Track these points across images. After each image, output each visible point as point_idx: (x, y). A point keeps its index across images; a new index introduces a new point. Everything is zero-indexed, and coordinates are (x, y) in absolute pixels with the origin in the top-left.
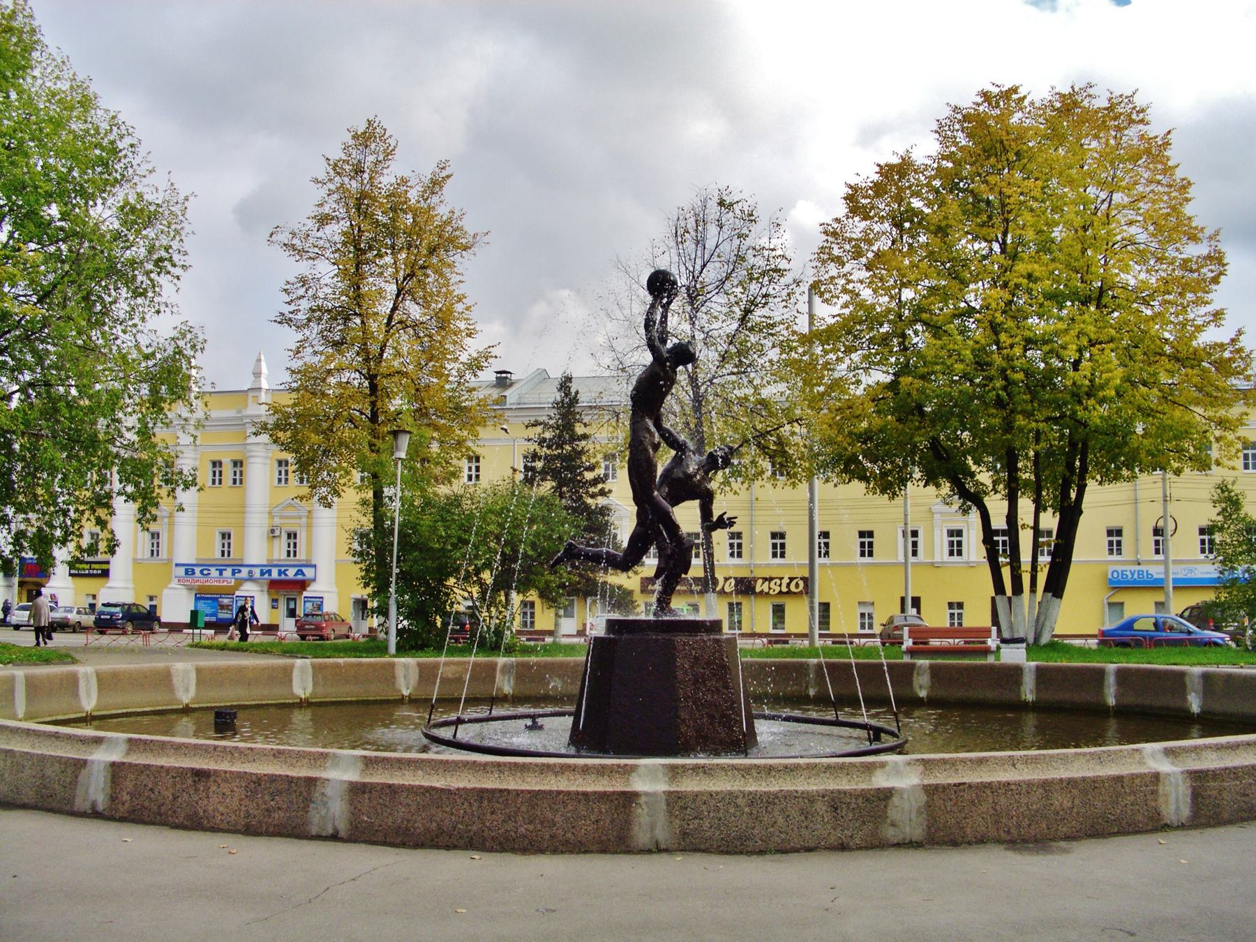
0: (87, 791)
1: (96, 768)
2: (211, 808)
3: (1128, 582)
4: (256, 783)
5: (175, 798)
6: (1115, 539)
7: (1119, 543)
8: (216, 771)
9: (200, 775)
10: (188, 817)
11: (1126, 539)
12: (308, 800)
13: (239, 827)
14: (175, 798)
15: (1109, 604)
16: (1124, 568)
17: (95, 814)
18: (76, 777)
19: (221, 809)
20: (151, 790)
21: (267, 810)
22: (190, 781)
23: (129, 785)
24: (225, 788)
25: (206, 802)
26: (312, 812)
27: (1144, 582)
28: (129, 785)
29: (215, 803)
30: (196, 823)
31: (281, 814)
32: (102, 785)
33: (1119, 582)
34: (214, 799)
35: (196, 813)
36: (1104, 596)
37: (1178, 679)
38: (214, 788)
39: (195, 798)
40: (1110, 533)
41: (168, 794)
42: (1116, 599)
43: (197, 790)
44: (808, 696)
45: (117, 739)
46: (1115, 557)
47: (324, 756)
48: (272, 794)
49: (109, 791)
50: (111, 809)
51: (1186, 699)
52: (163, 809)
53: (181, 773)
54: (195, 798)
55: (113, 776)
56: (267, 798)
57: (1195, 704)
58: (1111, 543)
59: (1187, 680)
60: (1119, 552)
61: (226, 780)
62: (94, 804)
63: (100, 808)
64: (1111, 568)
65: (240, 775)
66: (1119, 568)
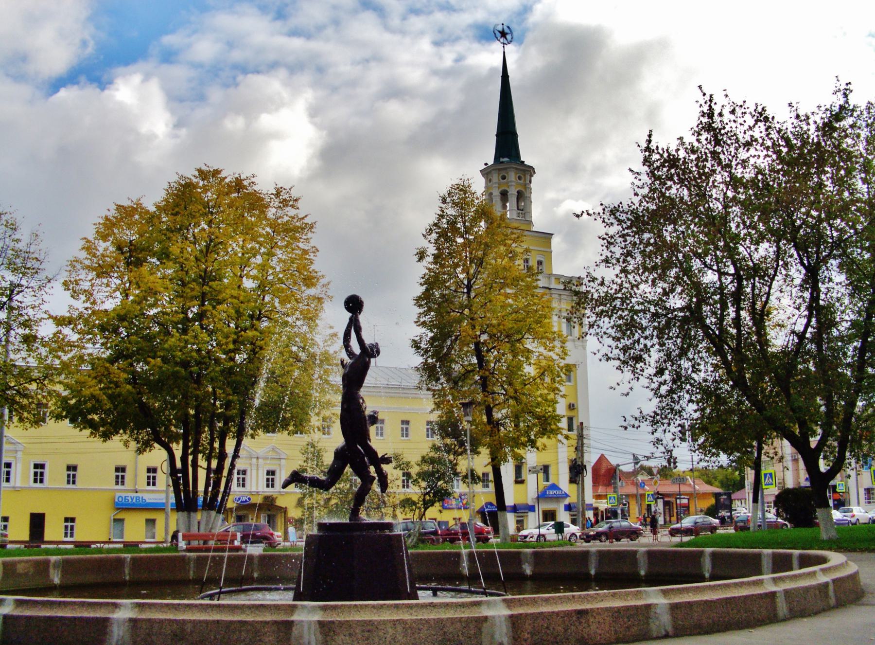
0: (492, 636)
1: (497, 621)
5: (566, 630)
6: (120, 474)
7: (123, 477)
8: (591, 609)
9: (581, 613)
11: (128, 475)
12: (648, 618)
18: (480, 629)
20: (547, 628)
23: (528, 627)
26: (652, 624)
28: (528, 627)
33: (122, 504)
34: (593, 627)
35: (583, 637)
36: (112, 514)
40: (117, 469)
41: (560, 629)
42: (118, 517)
43: (580, 623)
46: (120, 487)
51: (521, 568)
53: (568, 614)
54: (580, 628)
56: (626, 620)
57: (528, 570)
58: (117, 477)
59: (522, 557)
60: (123, 483)
64: (118, 494)
65: (607, 609)
66: (124, 495)
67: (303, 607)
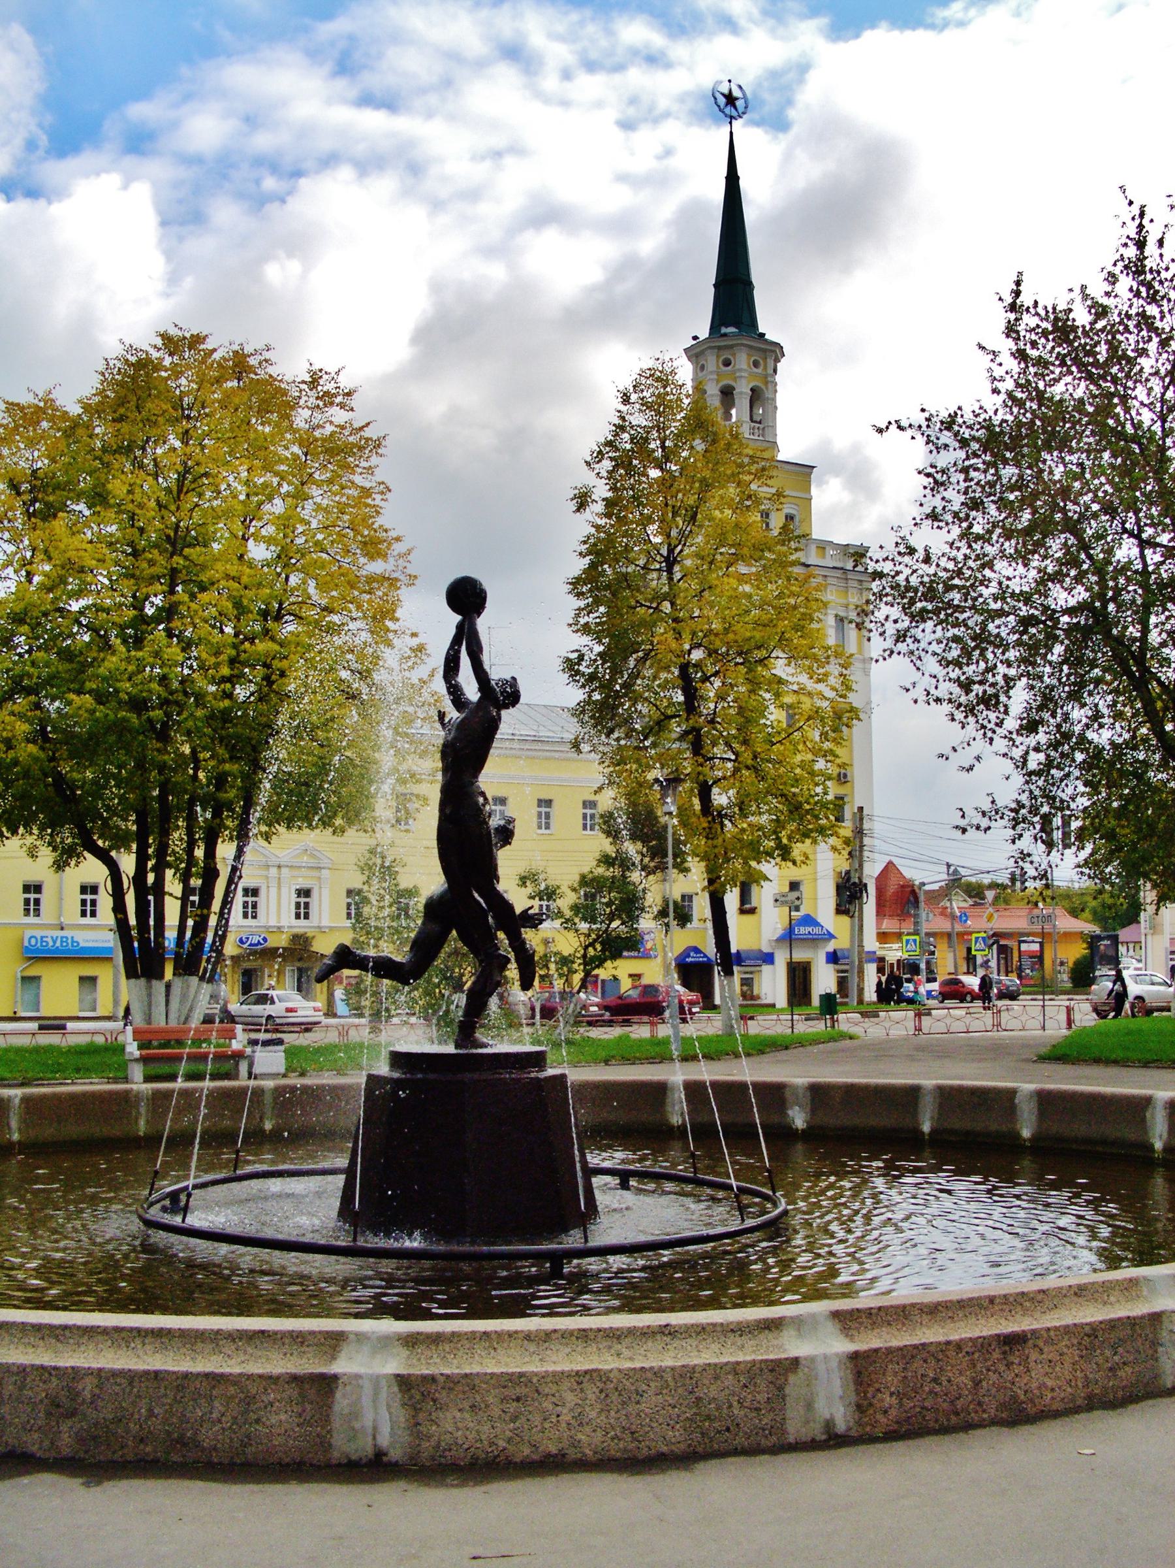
0: (809, 1406)
1: (821, 1368)
2: (1034, 1385)
3: (49, 951)
4: (1091, 1335)
5: (977, 1383)
6: (32, 896)
7: (37, 902)
8: (1034, 1331)
9: (1012, 1341)
10: (1003, 1406)
11: (46, 897)
12: (1155, 1344)
13: (1079, 1402)
14: (977, 1383)
15: (23, 978)
16: (44, 933)
17: (834, 1440)
18: (780, 1389)
19: (1050, 1383)
20: (935, 1380)
21: (1111, 1369)
22: (996, 1355)
23: (891, 1380)
24: (1050, 1353)
25: (1026, 1379)
26: (1163, 1359)
27: (69, 951)
28: (891, 1380)
29: (1042, 1377)
30: (1019, 1415)
31: (1128, 1369)
32: (839, 1392)
33: (38, 951)
34: (1038, 1372)
35: (1014, 1398)
36: (18, 968)
37: (660, 1090)
38: (1034, 1355)
39: (1009, 1376)
40: (27, 888)
41: (965, 1380)
42: (32, 972)
43: (1009, 1365)
44: (263, 1131)
45: (813, 1316)
46: (32, 919)
47: (1133, 1282)
48: (1114, 1348)
49: (853, 1398)
50: (859, 1423)
51: (786, 1115)
52: (959, 1404)
53: (983, 1345)
54: (1009, 1376)
55: (859, 1374)
56: (1108, 1353)
57: (799, 1119)
58: (27, 902)
59: (788, 1094)
60: (37, 913)
61: (1050, 1341)
62: (829, 1425)
63: (841, 1426)
64: (29, 933)
65: (1067, 1330)
66: (39, 933)
67: (361, 1337)
